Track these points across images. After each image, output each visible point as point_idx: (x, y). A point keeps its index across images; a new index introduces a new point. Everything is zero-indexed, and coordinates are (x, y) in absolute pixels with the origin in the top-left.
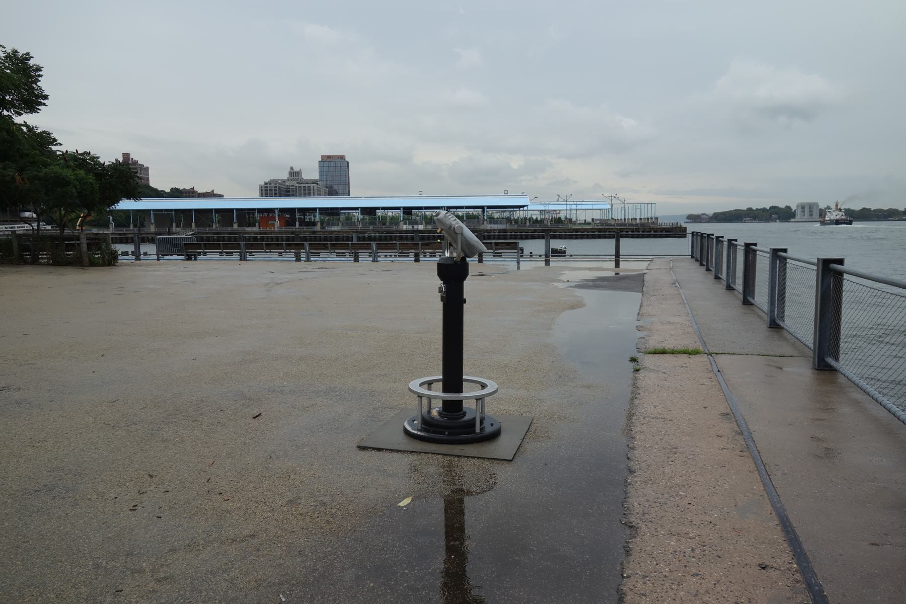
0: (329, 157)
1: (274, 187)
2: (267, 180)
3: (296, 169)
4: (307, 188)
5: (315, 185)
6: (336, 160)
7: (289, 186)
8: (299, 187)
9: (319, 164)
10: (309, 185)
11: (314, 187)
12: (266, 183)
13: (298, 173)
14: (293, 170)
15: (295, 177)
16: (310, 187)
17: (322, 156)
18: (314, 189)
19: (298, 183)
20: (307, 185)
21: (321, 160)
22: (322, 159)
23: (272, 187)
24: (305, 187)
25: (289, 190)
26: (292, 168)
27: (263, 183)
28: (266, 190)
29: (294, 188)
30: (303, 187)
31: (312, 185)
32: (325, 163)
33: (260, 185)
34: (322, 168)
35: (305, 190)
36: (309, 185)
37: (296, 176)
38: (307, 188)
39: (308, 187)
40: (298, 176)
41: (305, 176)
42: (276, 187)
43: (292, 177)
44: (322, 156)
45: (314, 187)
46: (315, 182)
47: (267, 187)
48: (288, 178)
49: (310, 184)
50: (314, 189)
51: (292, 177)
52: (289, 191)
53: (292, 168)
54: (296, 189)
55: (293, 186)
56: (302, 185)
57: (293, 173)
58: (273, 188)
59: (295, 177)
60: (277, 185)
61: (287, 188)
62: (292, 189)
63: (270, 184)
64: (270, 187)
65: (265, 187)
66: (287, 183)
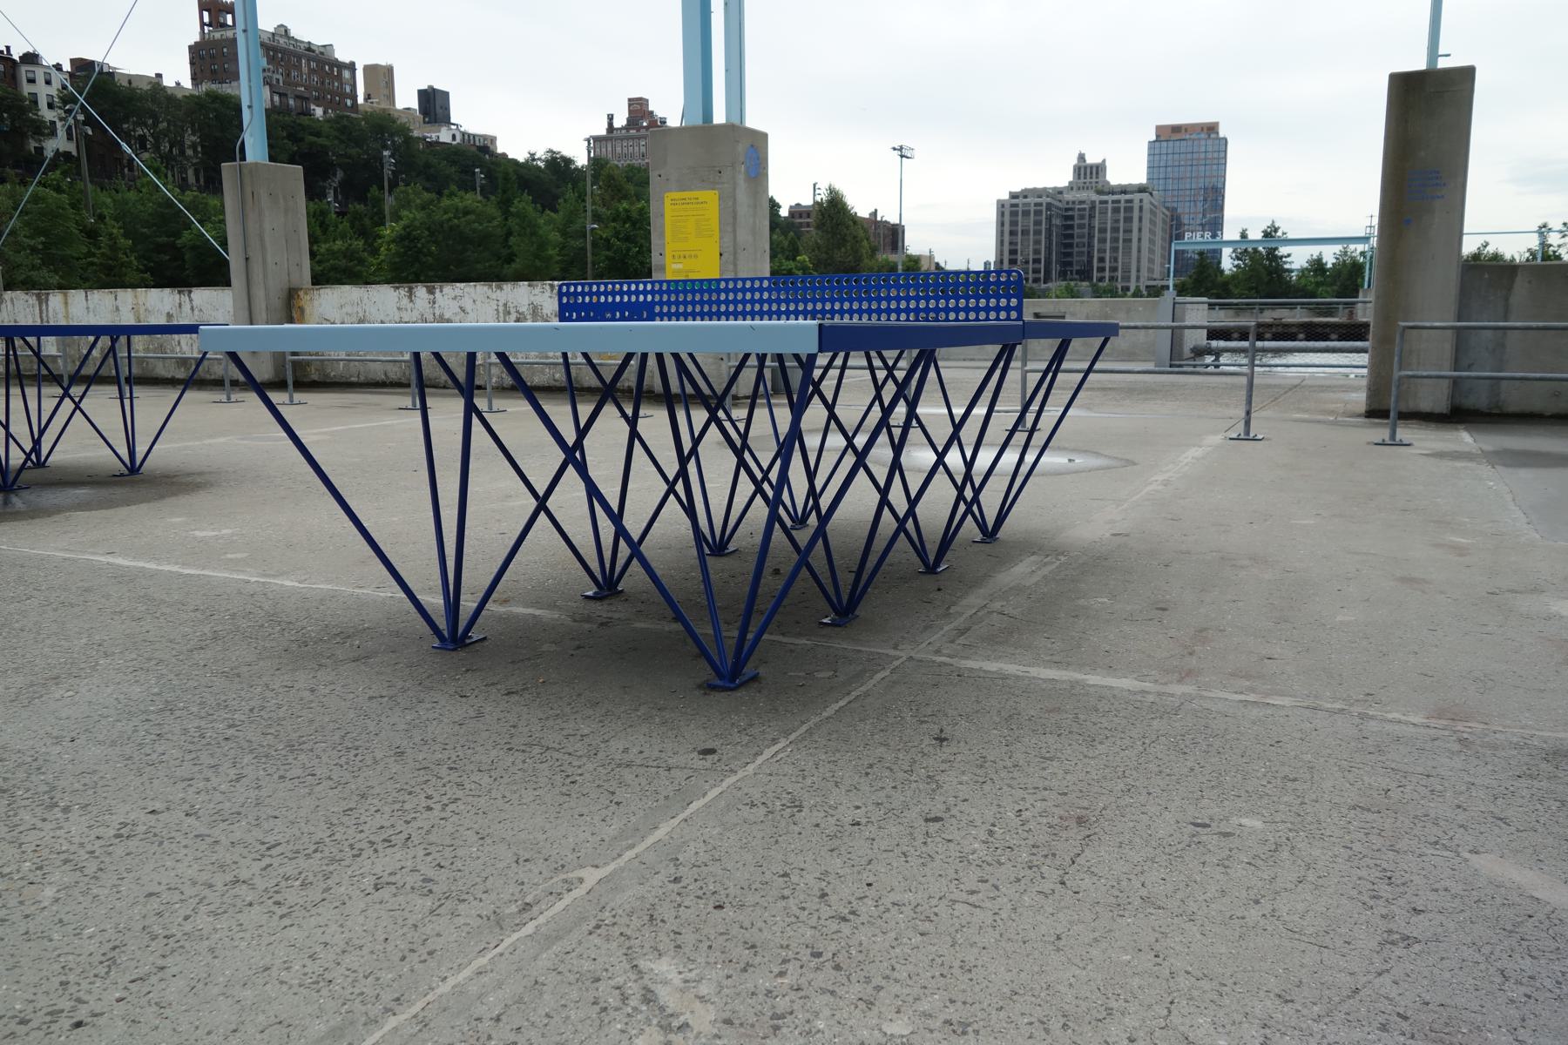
0: (1176, 129)
1: (1036, 205)
2: (1017, 189)
3: (1091, 159)
4: (1122, 205)
5: (1145, 196)
6: (1194, 136)
7: (1074, 203)
8: (1101, 202)
9: (1150, 148)
10: (1128, 197)
11: (1141, 201)
12: (1014, 196)
13: (1099, 169)
14: (1085, 161)
15: (1088, 180)
16: (1130, 201)
17: (1159, 129)
18: (1141, 209)
19: (1100, 192)
20: (1123, 197)
21: (1154, 138)
22: (1157, 136)
23: (1029, 204)
24: (1119, 202)
25: (1070, 213)
26: (1082, 157)
27: (1006, 197)
28: (1014, 214)
29: (1084, 209)
30: (1113, 202)
31: (1137, 196)
32: (1164, 144)
33: (998, 201)
34: (1157, 158)
35: (1116, 210)
36: (1128, 197)
37: (1091, 178)
38: (1122, 205)
39: (1128, 201)
40: (1097, 178)
41: (1114, 177)
42: (1041, 204)
43: (1082, 180)
44: (1159, 129)
45: (1141, 201)
46: (1141, 189)
47: (1016, 205)
48: (1070, 183)
49: (1132, 192)
50: (1141, 209)
51: (1082, 180)
52: (1072, 218)
53: (1082, 157)
54: (1093, 208)
55: (1082, 202)
56: (1110, 198)
57: (1085, 168)
58: (1032, 209)
59: (1088, 180)
60: (1044, 200)
61: (1067, 210)
62: (1079, 210)
63: (1025, 197)
64: (1024, 204)
65: (1013, 205)
66: (1068, 197)
